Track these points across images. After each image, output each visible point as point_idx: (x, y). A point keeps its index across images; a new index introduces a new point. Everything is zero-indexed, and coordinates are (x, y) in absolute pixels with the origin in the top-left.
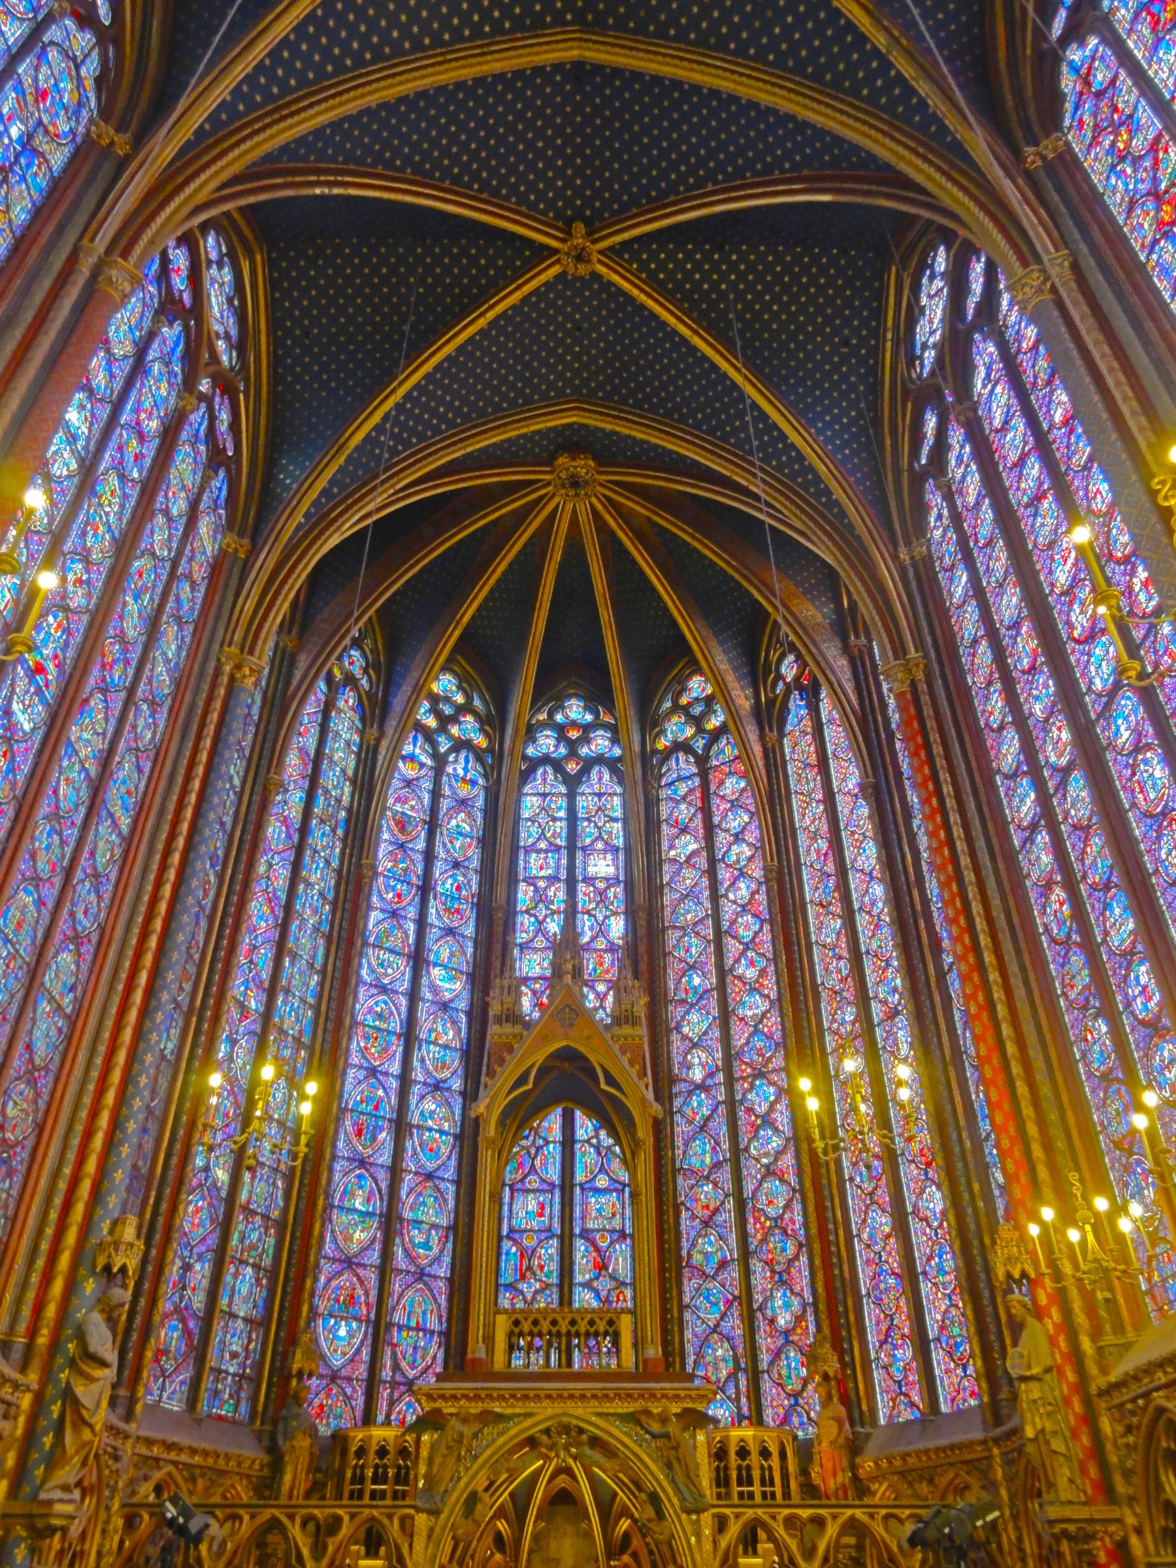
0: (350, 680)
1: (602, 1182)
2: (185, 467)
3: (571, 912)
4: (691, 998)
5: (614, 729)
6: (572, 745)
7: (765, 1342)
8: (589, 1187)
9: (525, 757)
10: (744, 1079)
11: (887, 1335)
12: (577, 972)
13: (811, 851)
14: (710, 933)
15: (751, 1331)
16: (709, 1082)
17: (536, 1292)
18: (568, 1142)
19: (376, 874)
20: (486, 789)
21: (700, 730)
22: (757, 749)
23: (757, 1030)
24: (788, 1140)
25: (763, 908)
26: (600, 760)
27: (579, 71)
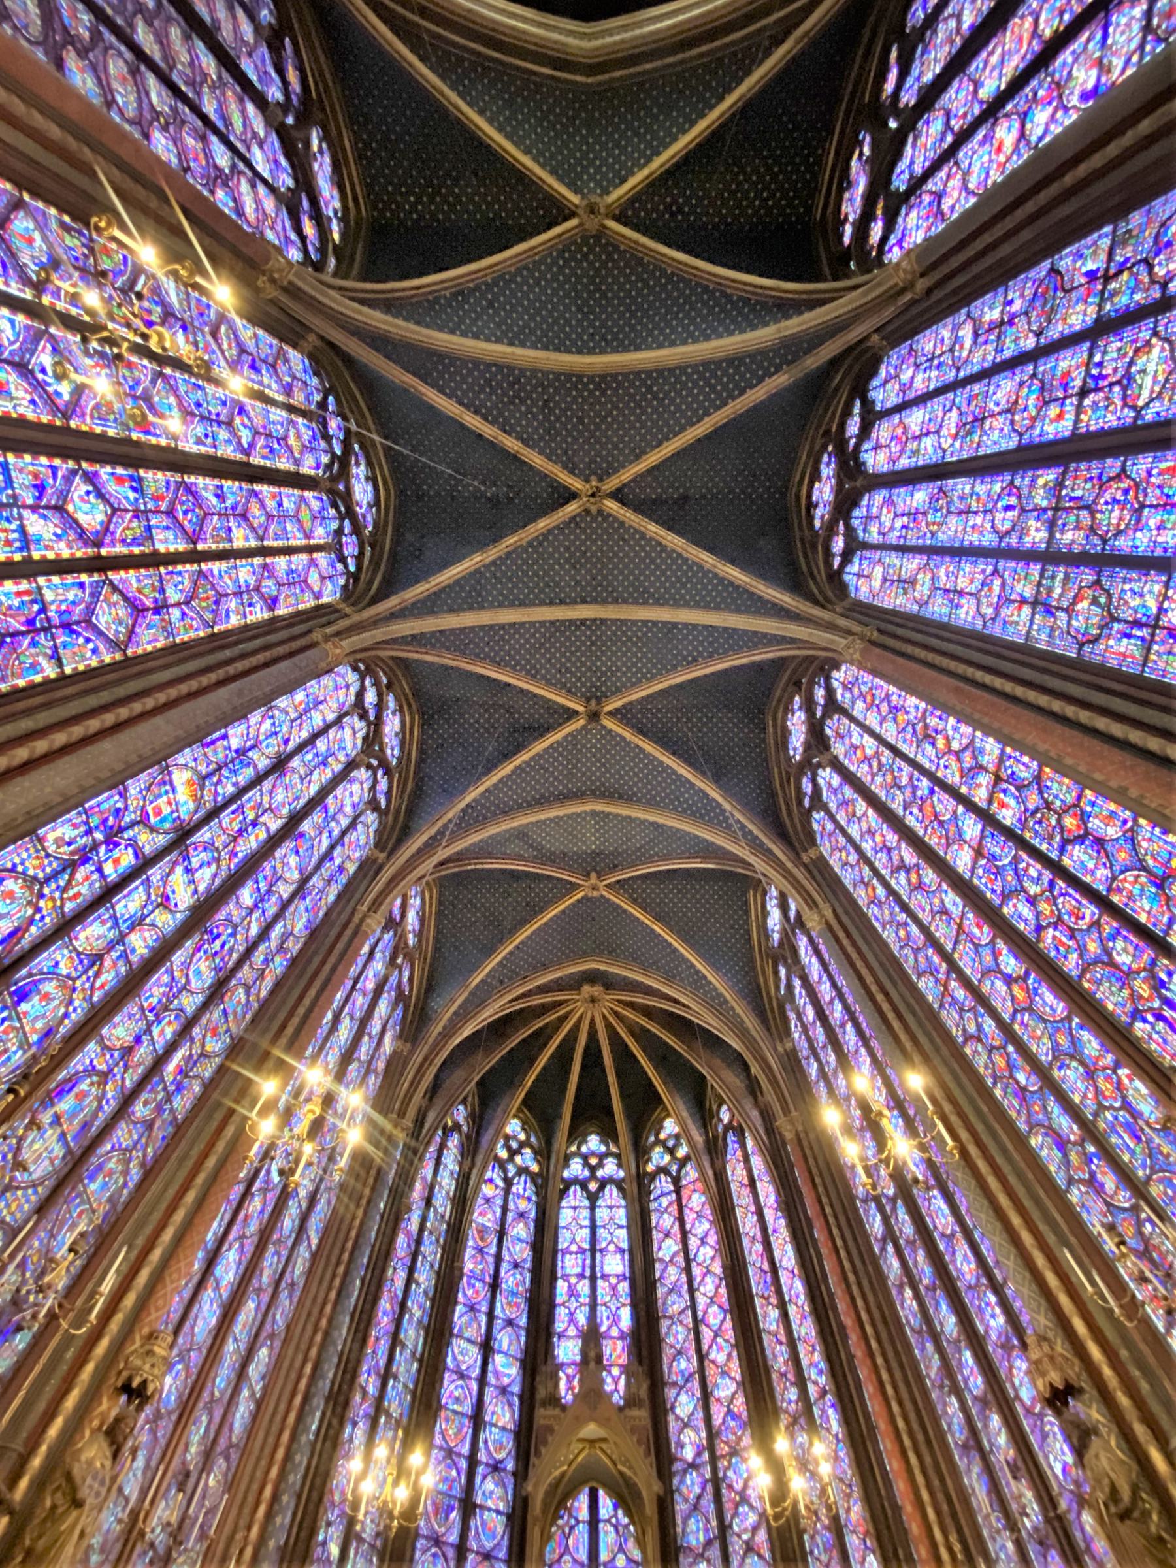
0: (457, 1127)
2: (383, 1007)
3: (593, 1306)
4: (681, 1382)
5: (618, 1156)
6: (593, 1169)
9: (563, 1180)
12: (599, 1358)
13: (753, 1253)
14: (689, 1321)
19: (461, 1275)
20: (538, 1204)
22: (710, 1173)
23: (729, 1412)
25: (724, 1299)
27: (594, 814)
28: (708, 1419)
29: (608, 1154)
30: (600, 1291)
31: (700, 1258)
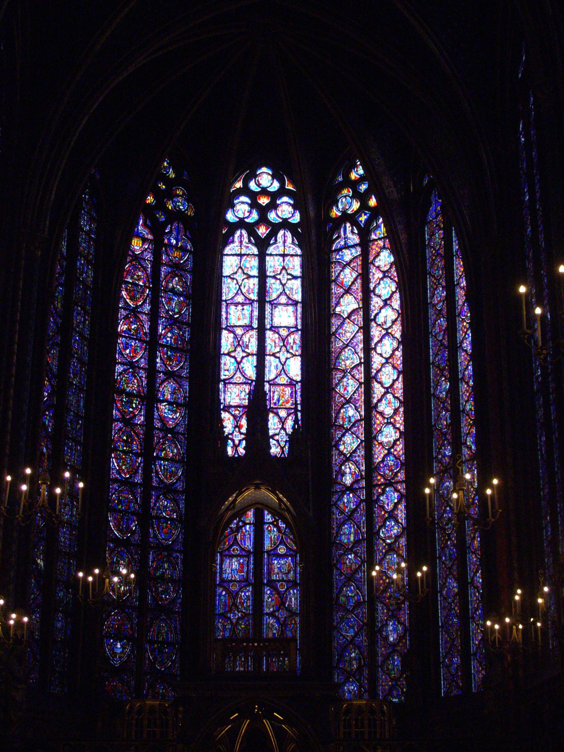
1: (282, 550)
3: (261, 354)
4: (347, 425)
6: (263, 211)
7: (382, 650)
8: (273, 554)
10: (379, 486)
11: (450, 649)
14: (361, 376)
15: (373, 643)
16: (356, 486)
17: (239, 619)
18: (259, 524)
21: (364, 207)
22: (403, 237)
24: (403, 528)
25: (399, 362)
26: (285, 224)
28: (369, 456)
29: (282, 192)
30: (268, 342)
31: (380, 320)
